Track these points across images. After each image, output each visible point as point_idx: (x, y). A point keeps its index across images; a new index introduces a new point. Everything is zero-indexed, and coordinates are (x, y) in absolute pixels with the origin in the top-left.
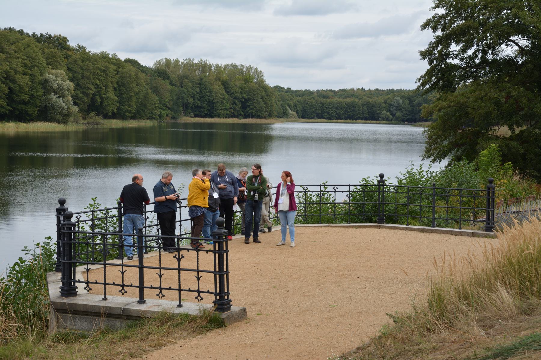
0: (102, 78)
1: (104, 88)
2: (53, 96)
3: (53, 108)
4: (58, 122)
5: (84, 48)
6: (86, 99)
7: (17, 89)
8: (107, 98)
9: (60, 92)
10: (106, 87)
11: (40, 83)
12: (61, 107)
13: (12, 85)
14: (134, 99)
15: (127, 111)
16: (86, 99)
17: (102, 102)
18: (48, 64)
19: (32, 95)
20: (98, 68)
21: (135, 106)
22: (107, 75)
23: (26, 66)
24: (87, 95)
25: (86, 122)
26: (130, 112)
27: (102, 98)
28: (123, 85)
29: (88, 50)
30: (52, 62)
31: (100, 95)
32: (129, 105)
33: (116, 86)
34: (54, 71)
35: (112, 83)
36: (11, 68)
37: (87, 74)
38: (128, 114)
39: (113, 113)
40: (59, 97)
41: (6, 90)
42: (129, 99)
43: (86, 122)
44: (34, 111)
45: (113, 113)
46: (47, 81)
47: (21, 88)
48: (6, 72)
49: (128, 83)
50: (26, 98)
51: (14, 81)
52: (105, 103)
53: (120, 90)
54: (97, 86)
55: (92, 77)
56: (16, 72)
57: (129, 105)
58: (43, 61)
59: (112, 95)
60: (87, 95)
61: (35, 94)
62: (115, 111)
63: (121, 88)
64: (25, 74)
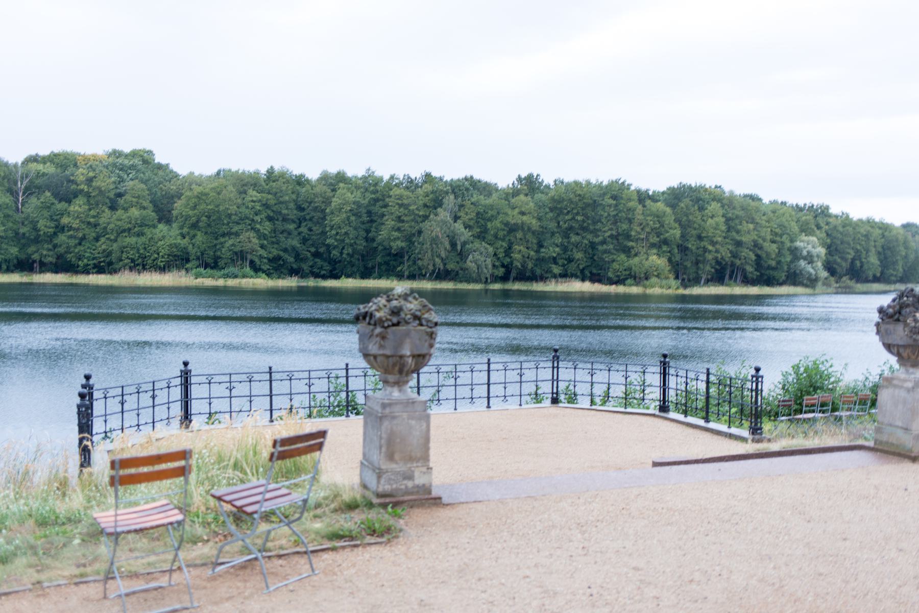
0: (863, 243)
1: (865, 252)
2: (802, 263)
3: (801, 274)
4: (806, 286)
5: (848, 216)
6: (844, 264)
7: (764, 256)
8: (868, 262)
9: (810, 259)
10: (867, 251)
11: (789, 249)
12: (809, 272)
13: (759, 252)
14: (901, 263)
15: (892, 275)
16: (844, 264)
17: (861, 267)
18: (802, 231)
19: (780, 261)
20: (859, 232)
21: (901, 270)
22: (868, 239)
23: (776, 234)
24: (845, 259)
25: (838, 285)
26: (896, 276)
27: (862, 263)
28: (889, 248)
29: (851, 216)
30: (805, 229)
31: (860, 260)
32: (894, 270)
33: (880, 249)
34: (806, 238)
35: (875, 246)
36: (760, 237)
37: (846, 239)
38: (893, 278)
39: (874, 276)
40: (809, 263)
41: (753, 257)
42: (895, 263)
43: (838, 285)
44: (783, 276)
45: (874, 276)
46: (796, 248)
47: (768, 254)
48: (755, 241)
49: (894, 247)
50: (773, 263)
51: (761, 248)
52: (866, 267)
53: (884, 254)
54: (857, 251)
55: (852, 243)
56: (764, 240)
57: (894, 270)
58: (796, 229)
59: (874, 260)
60: (845, 259)
61: (783, 260)
62: (878, 275)
63: (886, 252)
64: (773, 242)
